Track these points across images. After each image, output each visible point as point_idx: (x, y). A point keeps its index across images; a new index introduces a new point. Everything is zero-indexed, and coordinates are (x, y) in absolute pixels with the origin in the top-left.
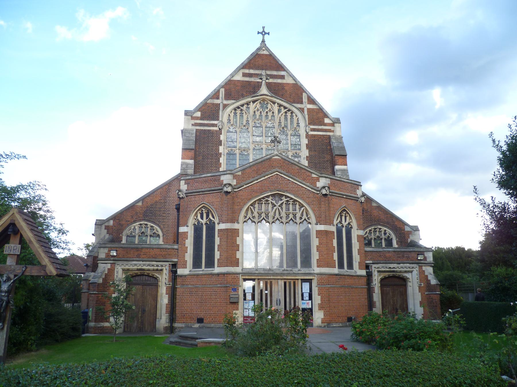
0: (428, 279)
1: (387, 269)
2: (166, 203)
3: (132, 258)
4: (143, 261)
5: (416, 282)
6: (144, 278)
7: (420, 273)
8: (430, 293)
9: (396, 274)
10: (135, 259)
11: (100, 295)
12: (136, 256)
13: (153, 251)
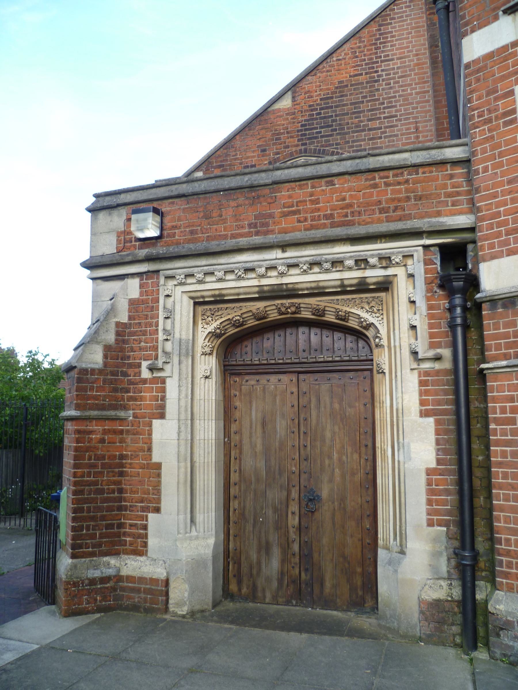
2: (376, 81)
3: (233, 237)
4: (284, 246)
6: (301, 336)
10: (243, 241)
11: (94, 426)
12: (250, 225)
13: (332, 192)
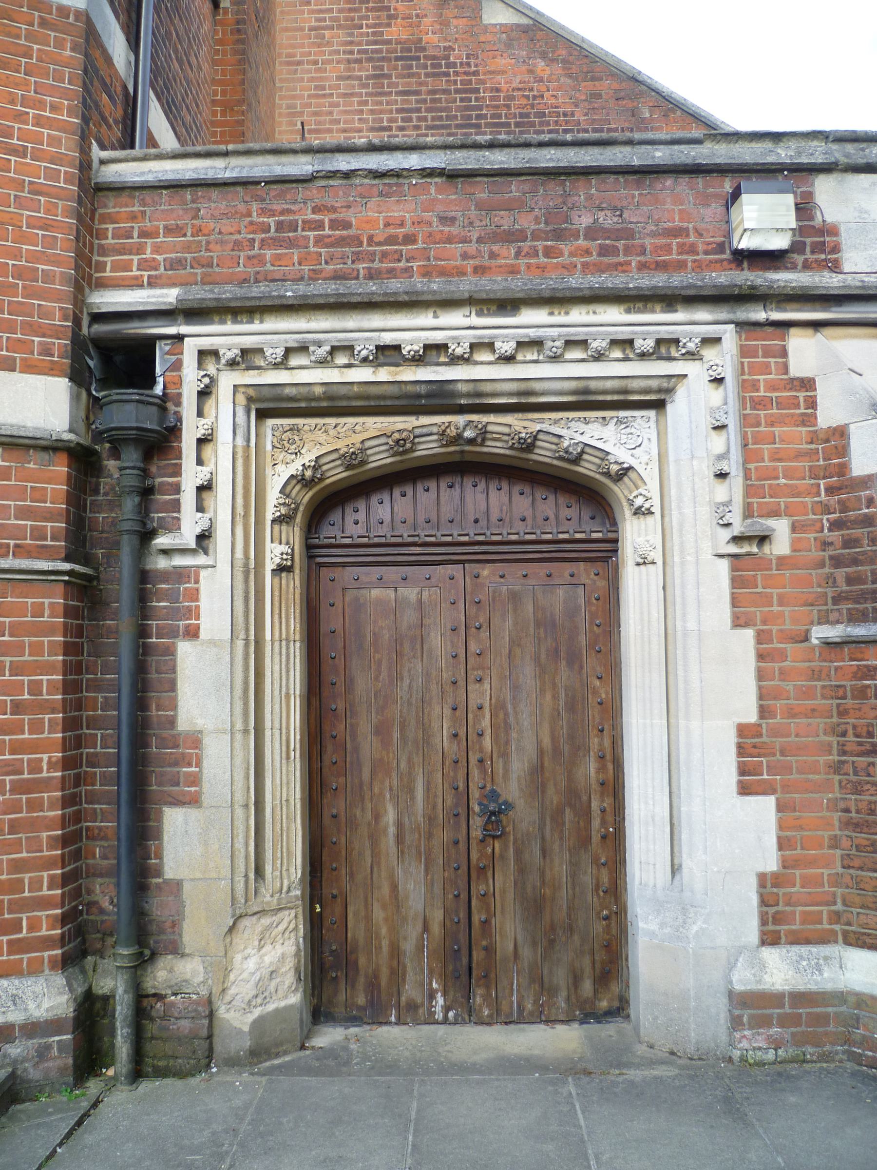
0: (843, 469)
1: (363, 374)
5: (705, 513)
7: (757, 404)
8: (860, 631)
9: (484, 434)
